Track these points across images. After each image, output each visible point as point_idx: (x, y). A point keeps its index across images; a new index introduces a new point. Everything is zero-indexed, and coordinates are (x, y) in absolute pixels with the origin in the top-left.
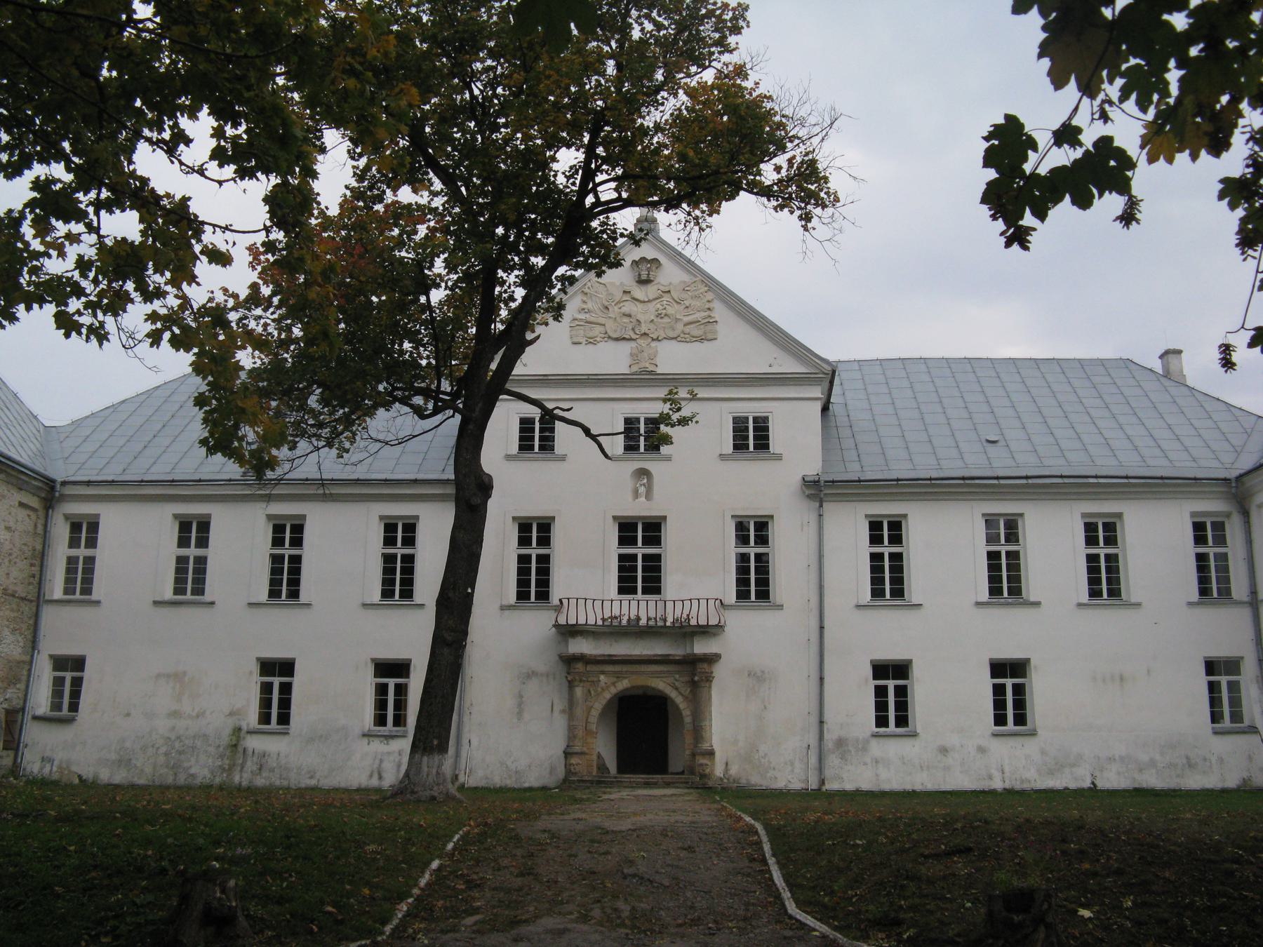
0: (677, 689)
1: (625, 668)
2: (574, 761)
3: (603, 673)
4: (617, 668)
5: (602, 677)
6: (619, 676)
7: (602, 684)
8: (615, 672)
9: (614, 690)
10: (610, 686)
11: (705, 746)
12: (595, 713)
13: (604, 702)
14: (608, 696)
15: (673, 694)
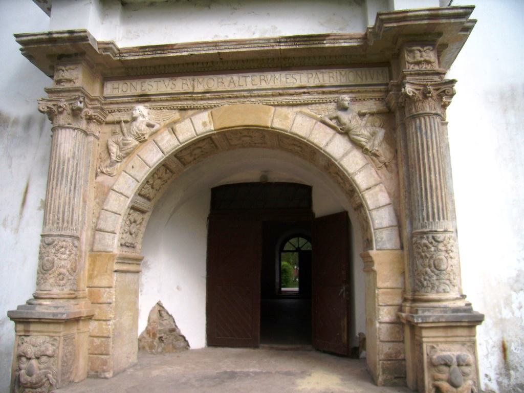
0: (345, 132)
1: (202, 84)
2: (39, 340)
3: (143, 98)
4: (181, 85)
5: (141, 109)
6: (185, 104)
7: (140, 125)
8: (176, 96)
9: (169, 143)
10: (162, 129)
11: (448, 298)
12: (119, 203)
13: (143, 174)
14: (153, 157)
15: (336, 147)
